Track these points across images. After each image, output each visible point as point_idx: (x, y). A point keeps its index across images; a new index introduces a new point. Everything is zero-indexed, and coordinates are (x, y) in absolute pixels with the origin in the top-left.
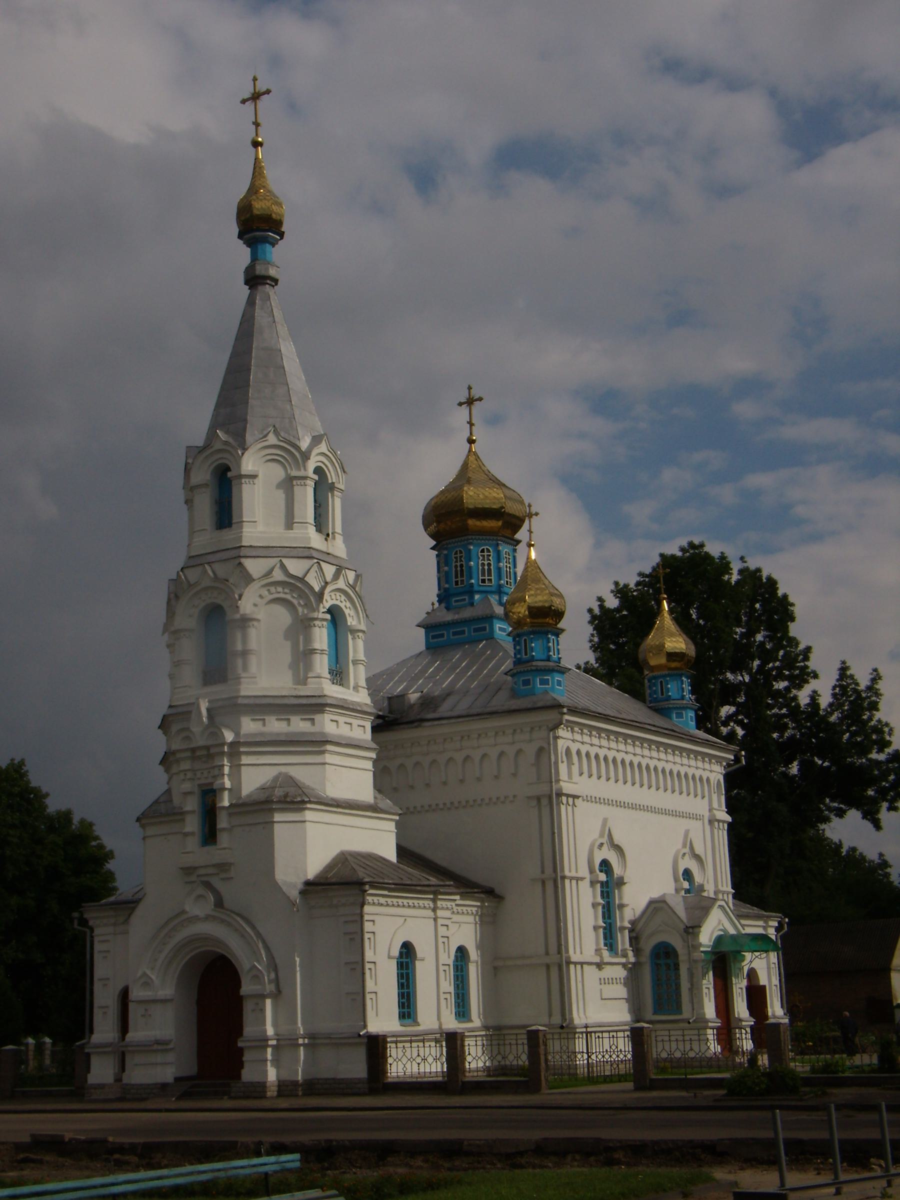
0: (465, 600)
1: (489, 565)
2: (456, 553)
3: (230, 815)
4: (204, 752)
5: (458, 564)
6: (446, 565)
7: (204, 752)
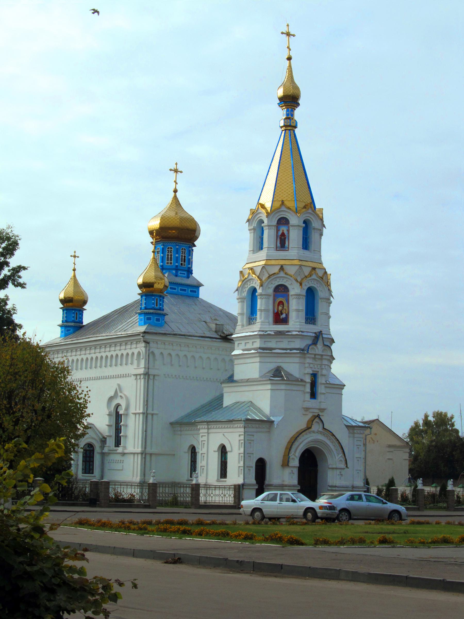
0: (184, 274)
1: (171, 255)
2: (168, 248)
3: (326, 387)
4: (320, 357)
5: (170, 254)
6: (177, 254)
7: (320, 357)
